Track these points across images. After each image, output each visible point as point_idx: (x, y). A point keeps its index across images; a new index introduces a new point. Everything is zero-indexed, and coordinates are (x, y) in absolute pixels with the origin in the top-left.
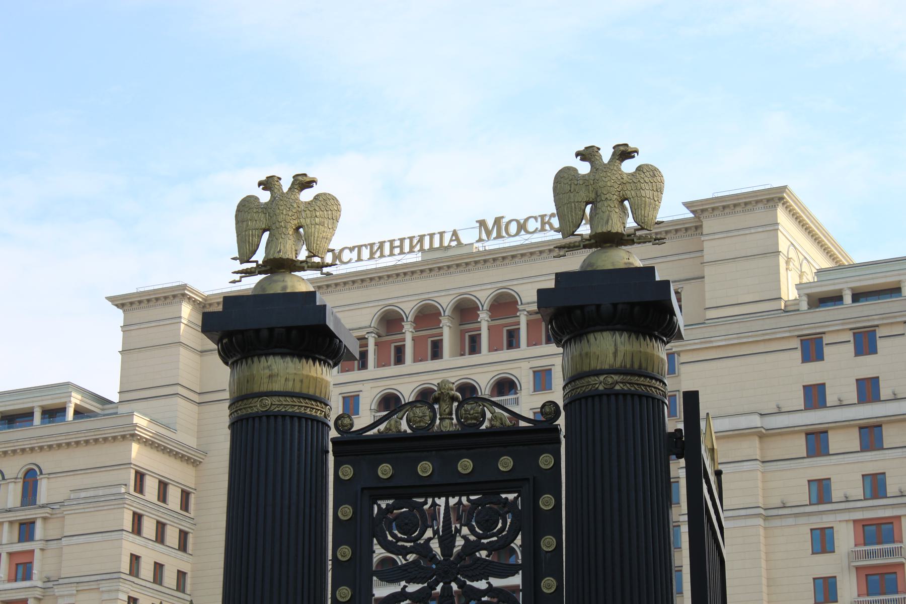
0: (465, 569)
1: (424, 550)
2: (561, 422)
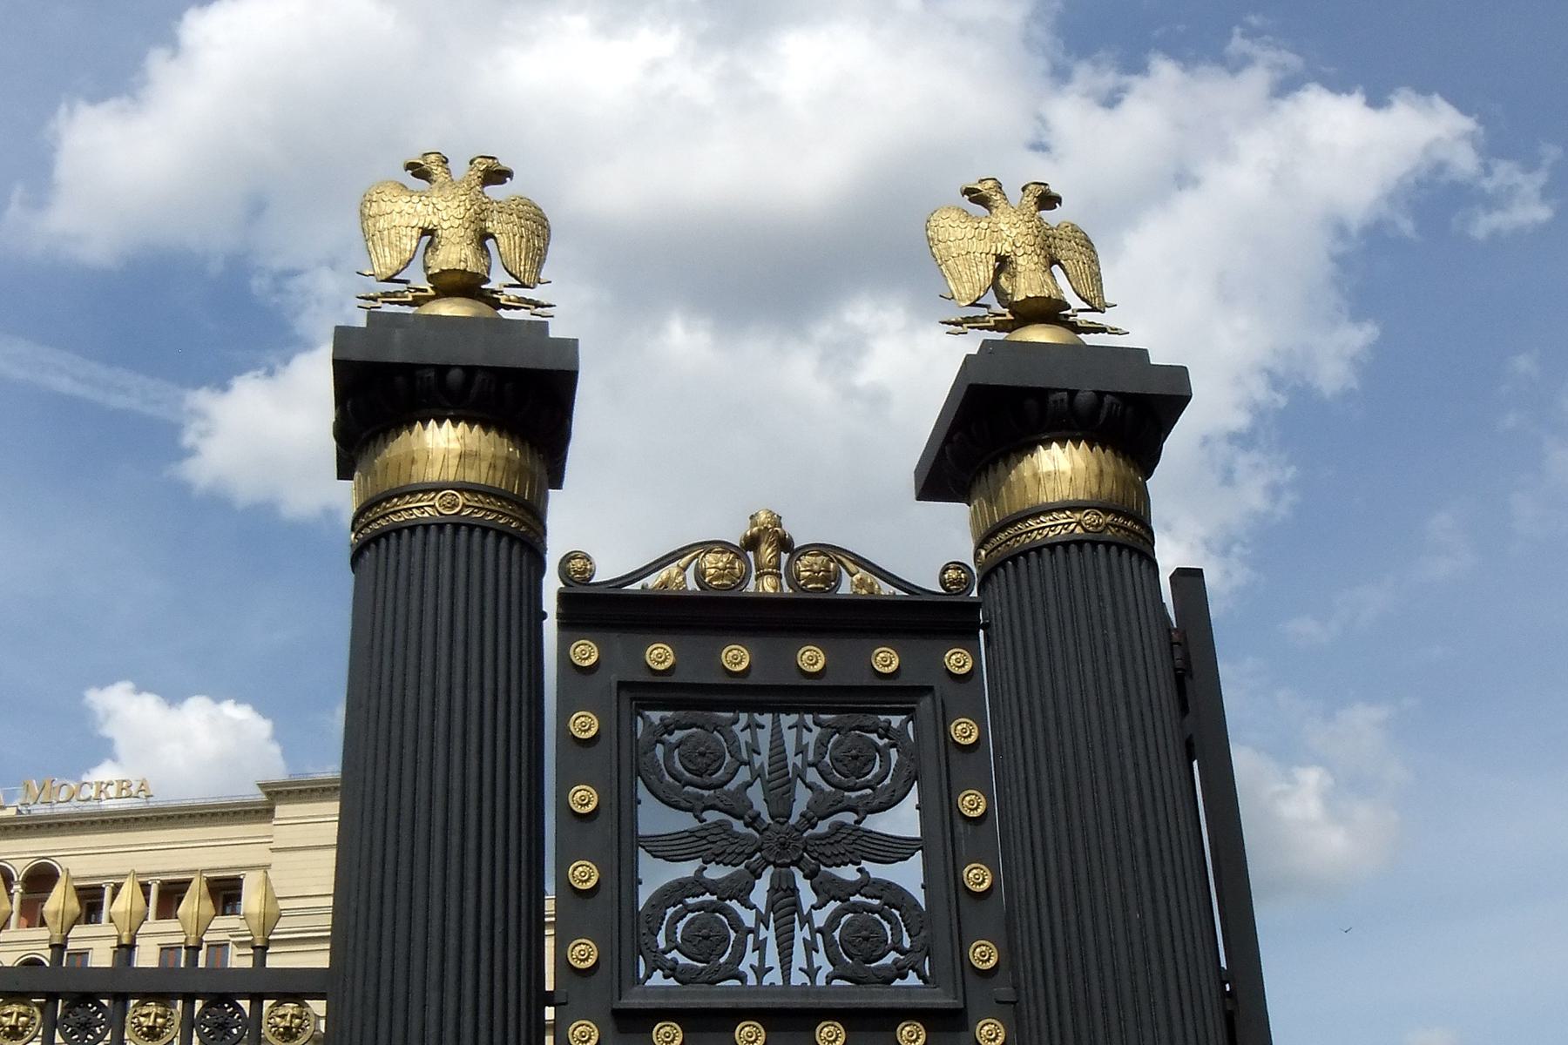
0: (818, 842)
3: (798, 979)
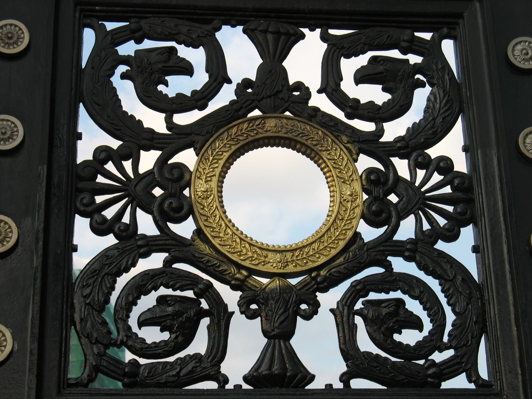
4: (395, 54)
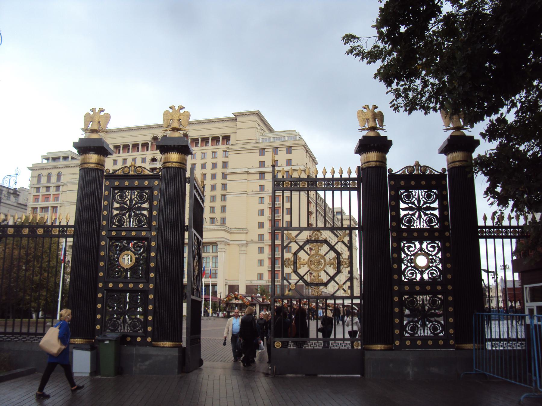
1: (413, 203)
2: (447, 173)
3: (422, 227)
4: (433, 245)
